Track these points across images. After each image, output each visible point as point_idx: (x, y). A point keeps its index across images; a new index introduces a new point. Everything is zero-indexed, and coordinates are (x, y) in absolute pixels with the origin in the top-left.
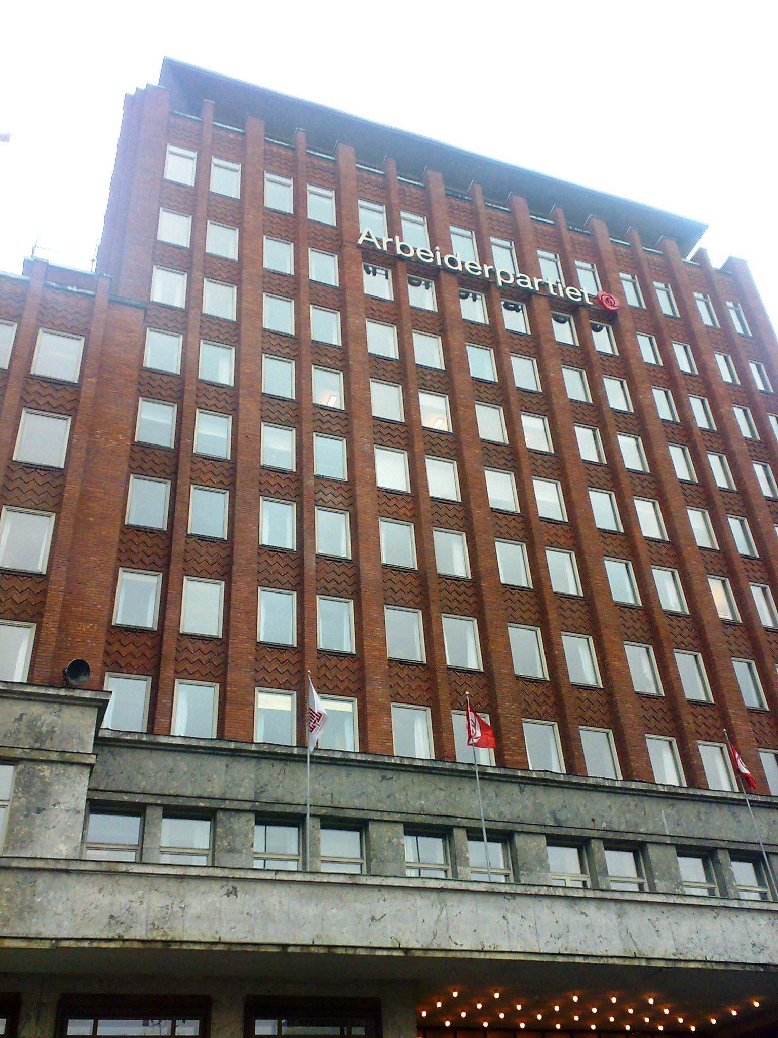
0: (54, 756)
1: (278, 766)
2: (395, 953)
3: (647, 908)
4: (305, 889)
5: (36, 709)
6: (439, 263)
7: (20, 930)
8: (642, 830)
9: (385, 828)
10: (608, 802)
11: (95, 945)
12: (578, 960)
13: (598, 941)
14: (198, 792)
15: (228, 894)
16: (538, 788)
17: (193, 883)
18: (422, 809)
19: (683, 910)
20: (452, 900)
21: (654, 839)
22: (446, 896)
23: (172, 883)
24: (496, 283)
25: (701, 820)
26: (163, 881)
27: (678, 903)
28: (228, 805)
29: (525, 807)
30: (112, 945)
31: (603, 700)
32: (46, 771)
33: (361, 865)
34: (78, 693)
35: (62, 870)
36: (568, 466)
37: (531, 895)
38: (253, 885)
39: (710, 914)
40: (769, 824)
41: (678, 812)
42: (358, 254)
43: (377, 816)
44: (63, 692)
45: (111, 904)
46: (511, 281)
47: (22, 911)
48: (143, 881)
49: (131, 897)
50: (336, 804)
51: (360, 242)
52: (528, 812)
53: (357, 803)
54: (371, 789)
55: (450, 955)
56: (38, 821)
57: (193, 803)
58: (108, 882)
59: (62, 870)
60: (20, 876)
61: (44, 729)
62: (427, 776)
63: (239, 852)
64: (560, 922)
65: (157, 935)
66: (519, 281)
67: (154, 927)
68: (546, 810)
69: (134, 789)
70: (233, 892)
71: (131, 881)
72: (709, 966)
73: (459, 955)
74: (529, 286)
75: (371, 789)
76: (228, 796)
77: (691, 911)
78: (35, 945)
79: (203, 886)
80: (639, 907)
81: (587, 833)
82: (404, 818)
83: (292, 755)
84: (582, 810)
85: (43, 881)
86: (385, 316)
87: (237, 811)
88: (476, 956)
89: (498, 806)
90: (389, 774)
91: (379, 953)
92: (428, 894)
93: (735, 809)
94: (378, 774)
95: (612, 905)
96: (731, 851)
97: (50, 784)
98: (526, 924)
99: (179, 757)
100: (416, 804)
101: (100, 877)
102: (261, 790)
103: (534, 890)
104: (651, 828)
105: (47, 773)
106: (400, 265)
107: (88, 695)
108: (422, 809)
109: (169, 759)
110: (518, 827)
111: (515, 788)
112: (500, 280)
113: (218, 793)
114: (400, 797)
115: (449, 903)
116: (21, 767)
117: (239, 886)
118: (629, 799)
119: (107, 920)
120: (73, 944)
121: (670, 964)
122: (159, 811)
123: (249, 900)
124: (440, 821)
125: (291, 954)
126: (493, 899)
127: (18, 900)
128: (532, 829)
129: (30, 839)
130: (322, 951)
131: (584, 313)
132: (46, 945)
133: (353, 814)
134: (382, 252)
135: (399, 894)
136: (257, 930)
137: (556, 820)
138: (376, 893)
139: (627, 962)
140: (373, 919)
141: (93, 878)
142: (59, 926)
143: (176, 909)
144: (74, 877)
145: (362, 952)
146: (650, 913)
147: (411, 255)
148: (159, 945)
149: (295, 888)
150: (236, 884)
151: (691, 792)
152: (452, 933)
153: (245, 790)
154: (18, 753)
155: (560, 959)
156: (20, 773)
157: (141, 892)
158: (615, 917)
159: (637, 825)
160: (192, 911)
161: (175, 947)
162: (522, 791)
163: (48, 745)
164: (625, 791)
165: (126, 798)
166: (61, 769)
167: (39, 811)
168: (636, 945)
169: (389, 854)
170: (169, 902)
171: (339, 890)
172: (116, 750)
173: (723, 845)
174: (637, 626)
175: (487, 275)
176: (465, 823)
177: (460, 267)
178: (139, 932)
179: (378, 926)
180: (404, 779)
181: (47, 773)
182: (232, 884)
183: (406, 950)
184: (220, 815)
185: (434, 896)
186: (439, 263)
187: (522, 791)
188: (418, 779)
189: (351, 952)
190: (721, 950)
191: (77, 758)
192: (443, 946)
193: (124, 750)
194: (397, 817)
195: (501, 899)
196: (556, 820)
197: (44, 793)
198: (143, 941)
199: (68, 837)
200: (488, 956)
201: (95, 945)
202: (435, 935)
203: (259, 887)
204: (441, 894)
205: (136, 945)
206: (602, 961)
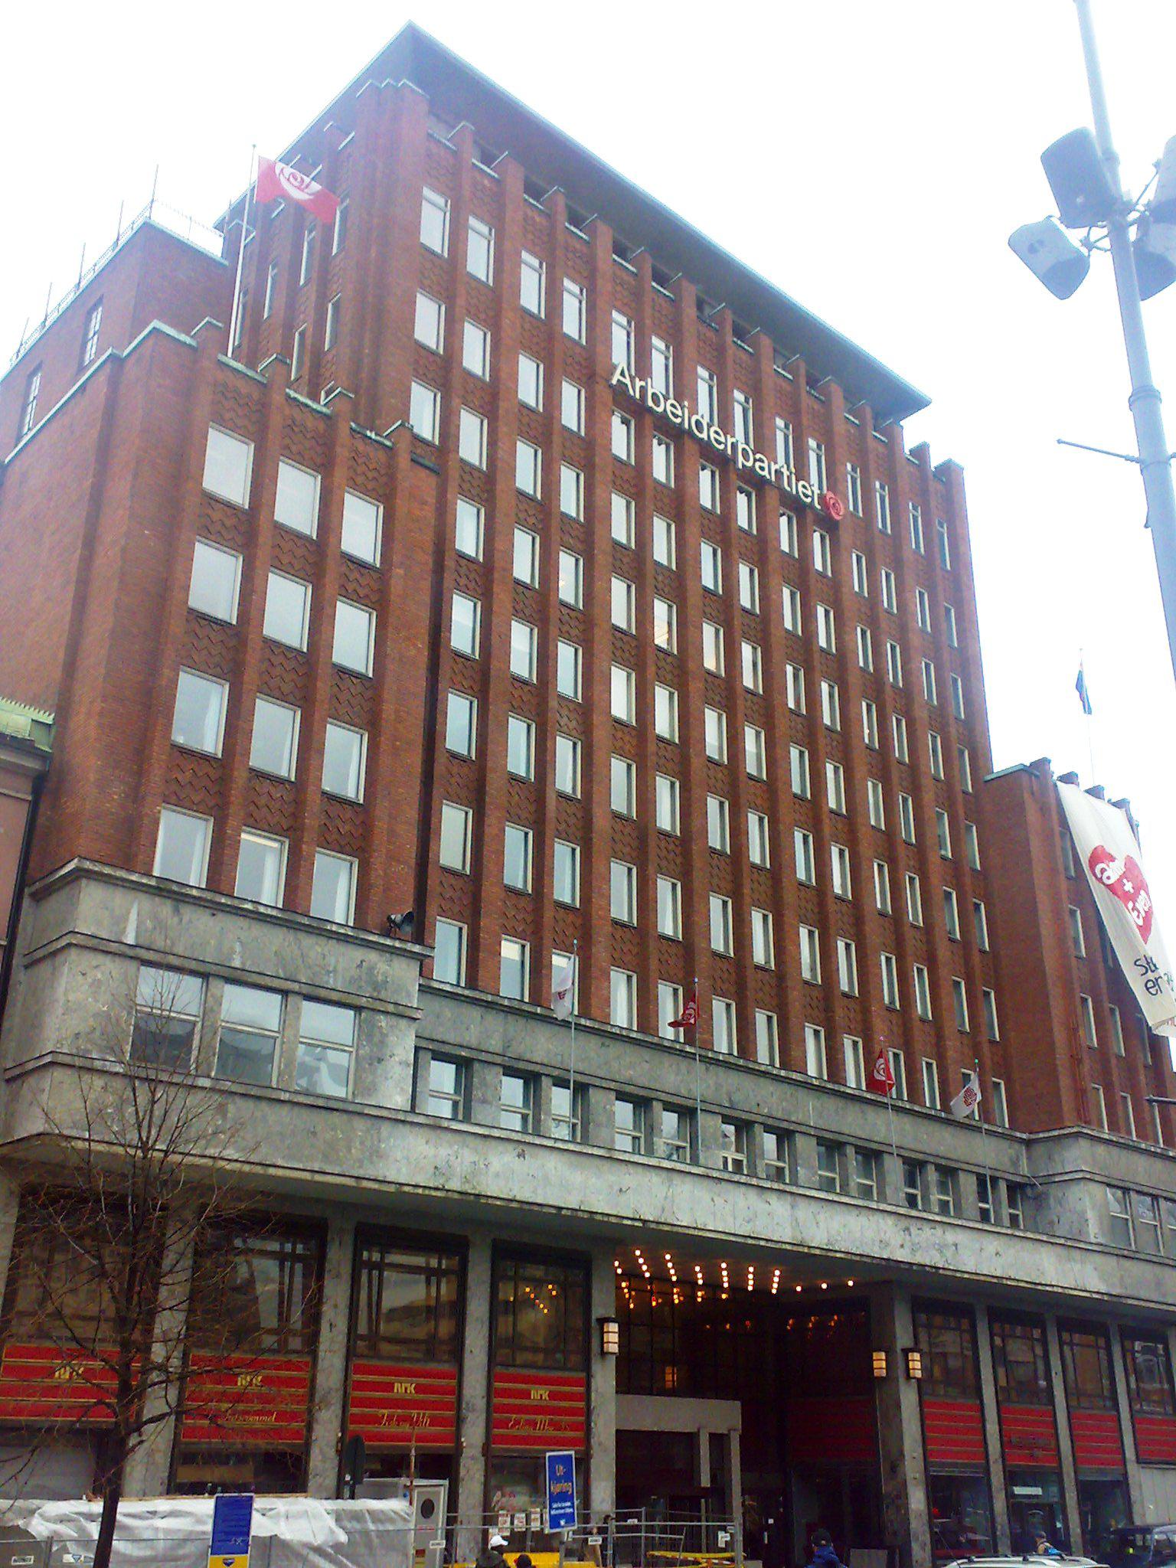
0: (391, 1008)
1: (522, 1021)
3: (812, 1202)
4: (573, 1157)
5: (372, 956)
6: (686, 426)
7: (371, 1173)
11: (427, 1192)
12: (762, 1243)
14: (458, 1041)
15: (519, 1156)
17: (494, 1143)
19: (836, 1206)
22: (675, 1176)
24: (735, 462)
28: (483, 1057)
29: (709, 1087)
30: (439, 1194)
31: (773, 982)
32: (383, 1021)
33: (574, 1125)
36: (777, 714)
39: (855, 1212)
42: (608, 396)
43: (597, 1082)
45: (435, 1156)
46: (749, 464)
47: (371, 1156)
48: (458, 1137)
51: (614, 382)
54: (593, 1054)
55: (675, 1229)
56: (379, 1071)
58: (432, 1135)
60: (369, 1122)
61: (380, 978)
66: (758, 464)
67: (468, 1181)
68: (724, 1090)
71: (449, 1136)
72: (849, 1257)
73: (680, 1230)
74: (765, 473)
75: (593, 1054)
77: (843, 1208)
78: (385, 1188)
79: (501, 1147)
80: (807, 1200)
81: (753, 1118)
85: (386, 1128)
86: (626, 486)
88: (691, 1232)
90: (607, 1041)
91: (626, 1222)
93: (865, 1107)
95: (789, 1198)
96: (856, 1146)
97: (386, 1035)
98: (728, 1207)
100: (627, 1074)
105: (383, 1024)
106: (648, 420)
112: (741, 459)
113: (474, 1043)
114: (615, 1065)
121: (824, 1253)
122: (429, 1055)
124: (642, 1092)
126: (706, 1182)
127: (368, 1143)
129: (371, 1089)
131: (810, 517)
132: (392, 1189)
134: (633, 398)
135: (640, 1169)
136: (540, 1191)
138: (623, 1166)
139: (795, 1248)
142: (399, 1170)
144: (408, 1127)
145: (613, 1220)
146: (815, 1206)
147: (660, 410)
150: (526, 1148)
151: (829, 1086)
153: (495, 1044)
154: (363, 1002)
155: (750, 1241)
163: (383, 996)
164: (777, 1078)
166: (394, 1020)
167: (380, 1060)
169: (603, 1119)
171: (597, 1162)
173: (851, 1140)
174: (809, 907)
175: (729, 451)
176: (663, 1097)
177: (704, 436)
178: (455, 1184)
179: (623, 1198)
183: (644, 1222)
184: (477, 1066)
185: (664, 1174)
186: (686, 426)
188: (629, 1049)
190: (858, 1243)
191: (409, 1013)
192: (670, 1221)
194: (613, 1085)
195: (711, 1183)
197: (382, 1043)
201: (427, 1192)
203: (542, 1152)
204: (670, 1174)
205: (456, 1196)
206: (777, 1246)
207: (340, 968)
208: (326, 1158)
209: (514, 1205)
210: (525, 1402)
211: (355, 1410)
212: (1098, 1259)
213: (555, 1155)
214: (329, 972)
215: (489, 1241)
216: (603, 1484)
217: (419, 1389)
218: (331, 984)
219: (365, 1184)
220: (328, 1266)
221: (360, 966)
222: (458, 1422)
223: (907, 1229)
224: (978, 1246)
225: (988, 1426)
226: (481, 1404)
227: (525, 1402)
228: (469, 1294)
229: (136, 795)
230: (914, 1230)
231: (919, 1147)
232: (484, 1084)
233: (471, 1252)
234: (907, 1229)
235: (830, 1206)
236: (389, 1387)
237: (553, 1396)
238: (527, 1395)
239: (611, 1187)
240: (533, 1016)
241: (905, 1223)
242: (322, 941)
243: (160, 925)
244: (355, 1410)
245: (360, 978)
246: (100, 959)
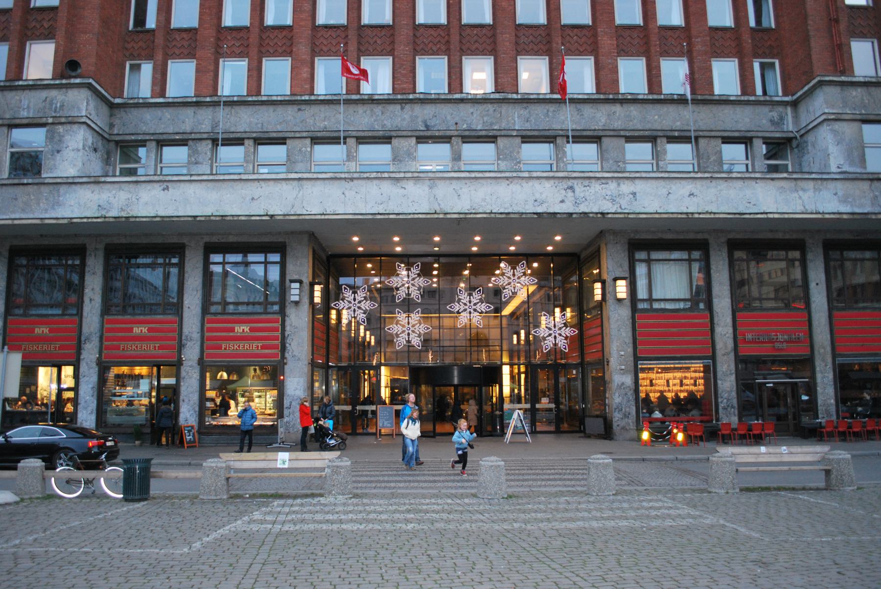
0: (63, 120)
2: (264, 218)
4: (210, 184)
5: (54, 93)
8: (495, 128)
10: (471, 110)
13: (410, 204)
14: (177, 130)
16: (416, 105)
17: (144, 185)
18: (325, 128)
20: (307, 185)
21: (503, 133)
22: (304, 182)
23: (131, 185)
25: (548, 116)
26: (127, 185)
27: (476, 177)
28: (193, 136)
29: (404, 119)
30: (99, 220)
32: (61, 129)
34: (73, 81)
35: (71, 183)
37: (364, 178)
38: (178, 184)
40: (609, 115)
41: (530, 112)
43: (292, 135)
44: (64, 81)
47: (53, 205)
48: (116, 186)
49: (109, 195)
50: (265, 130)
52: (405, 123)
53: (279, 128)
55: (301, 217)
57: (173, 137)
59: (71, 183)
60: (51, 187)
62: (331, 106)
63: (201, 163)
64: (384, 195)
65: (124, 214)
68: (420, 120)
69: (139, 132)
70: (167, 188)
72: (493, 215)
73: (307, 217)
76: (195, 131)
79: (149, 186)
82: (310, 134)
83: (234, 102)
84: (449, 117)
85: (63, 189)
87: (201, 139)
89: (383, 121)
90: (303, 107)
92: (291, 182)
94: (296, 108)
97: (63, 136)
99: (164, 110)
100: (321, 125)
101: (92, 185)
103: (365, 175)
104: (504, 125)
105: (61, 130)
107: (78, 81)
108: (325, 128)
110: (394, 134)
111: (398, 107)
113: (188, 130)
115: (305, 187)
116: (48, 127)
117: (169, 185)
118: (490, 106)
119: (96, 207)
120: (78, 220)
123: (176, 192)
125: (200, 221)
126: (337, 183)
127: (51, 199)
128: (404, 133)
130: (218, 219)
132: (66, 221)
133: (274, 135)
135: (272, 183)
137: (427, 126)
139: (429, 216)
140: (253, 199)
141: (89, 186)
143: (134, 199)
145: (243, 218)
148: (123, 219)
149: (204, 184)
150: (168, 184)
152: (305, 205)
153: (206, 127)
155: (379, 217)
156: (47, 131)
157: (114, 192)
158: (427, 189)
160: (142, 201)
161: (132, 220)
162: (402, 108)
165: (133, 138)
166: (68, 127)
167: (58, 152)
168: (439, 205)
170: (130, 196)
172: (127, 110)
173: (561, 133)
176: (354, 134)
178: (114, 213)
180: (315, 109)
181: (61, 130)
182: (166, 184)
183: (272, 216)
185: (295, 183)
187: (402, 108)
188: (323, 108)
189: (236, 218)
190: (507, 205)
191: (76, 120)
193: (132, 109)
194: (304, 134)
196: (427, 126)
197: (60, 141)
198: (115, 218)
199: (74, 165)
200: (326, 217)
201: (90, 220)
202: (293, 206)
203: (182, 185)
205: (111, 220)
206: (410, 217)
207: (31, 105)
208: (23, 210)
209: (158, 219)
210: (231, 334)
211: (106, 343)
212: (839, 185)
213: (198, 185)
214: (24, 109)
215: (202, 244)
216: (296, 380)
217: (150, 330)
219: (47, 221)
220: (87, 269)
221: (45, 100)
222: (181, 346)
223: (571, 188)
225: (718, 330)
226: (196, 336)
227: (231, 334)
228: (186, 275)
231: (648, 126)
233: (187, 252)
234: (571, 188)
235: (475, 183)
236: (131, 330)
237: (251, 330)
238: (233, 330)
239: (244, 198)
240: (254, 103)
242: (20, 93)
244: (106, 343)
245: (45, 107)
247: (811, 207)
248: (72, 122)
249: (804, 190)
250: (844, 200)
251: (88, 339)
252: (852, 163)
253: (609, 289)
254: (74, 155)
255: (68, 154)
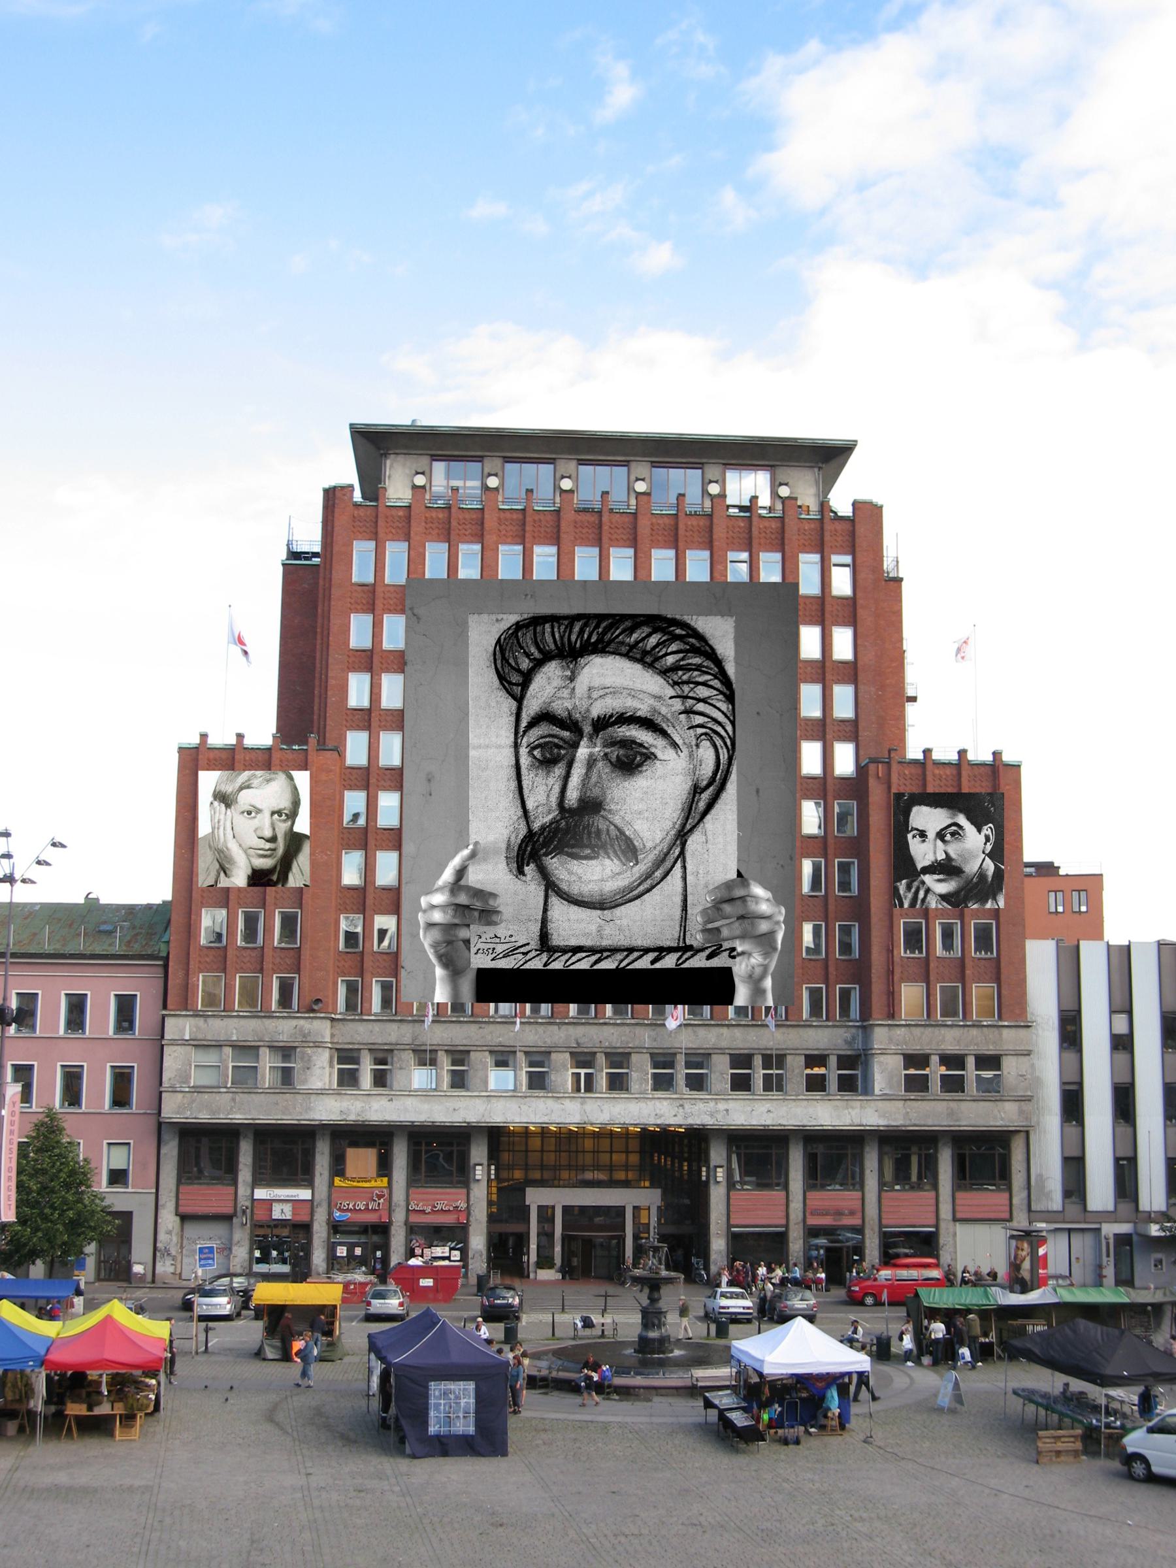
5: (302, 1022)
9: (478, 1054)
20: (494, 1100)
32: (309, 1051)
35: (321, 1093)
53: (465, 1042)
58: (338, 1097)
59: (321, 1093)
79: (378, 1098)
85: (313, 1097)
99: (374, 1024)
102: (415, 1038)
104: (637, 1044)
109: (370, 1026)
111: (556, 1027)
153: (407, 1039)
159: (628, 1043)
208: (283, 1113)
218: (281, 1038)
223: (682, 1105)
224: (749, 1109)
225: (792, 1205)
226: (403, 1204)
229: (187, 974)
230: (686, 1106)
232: (400, 1059)
241: (678, 1103)
243: (198, 1028)
246: (176, 1048)
247: (857, 1121)
248: (318, 1045)
249: (852, 1108)
250: (883, 1116)
251: (319, 1204)
252: (891, 1088)
253: (712, 1173)
254: (321, 1071)
255: (316, 1071)
